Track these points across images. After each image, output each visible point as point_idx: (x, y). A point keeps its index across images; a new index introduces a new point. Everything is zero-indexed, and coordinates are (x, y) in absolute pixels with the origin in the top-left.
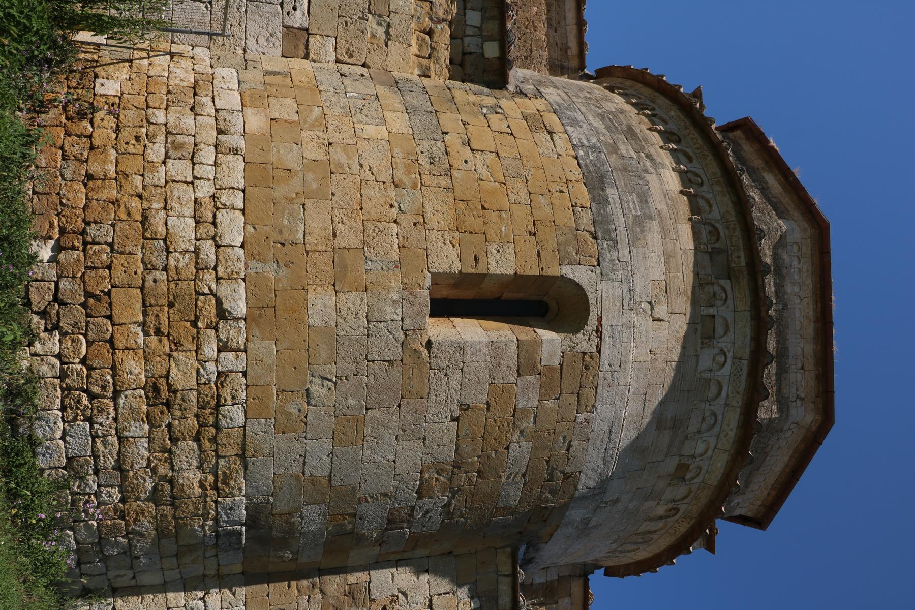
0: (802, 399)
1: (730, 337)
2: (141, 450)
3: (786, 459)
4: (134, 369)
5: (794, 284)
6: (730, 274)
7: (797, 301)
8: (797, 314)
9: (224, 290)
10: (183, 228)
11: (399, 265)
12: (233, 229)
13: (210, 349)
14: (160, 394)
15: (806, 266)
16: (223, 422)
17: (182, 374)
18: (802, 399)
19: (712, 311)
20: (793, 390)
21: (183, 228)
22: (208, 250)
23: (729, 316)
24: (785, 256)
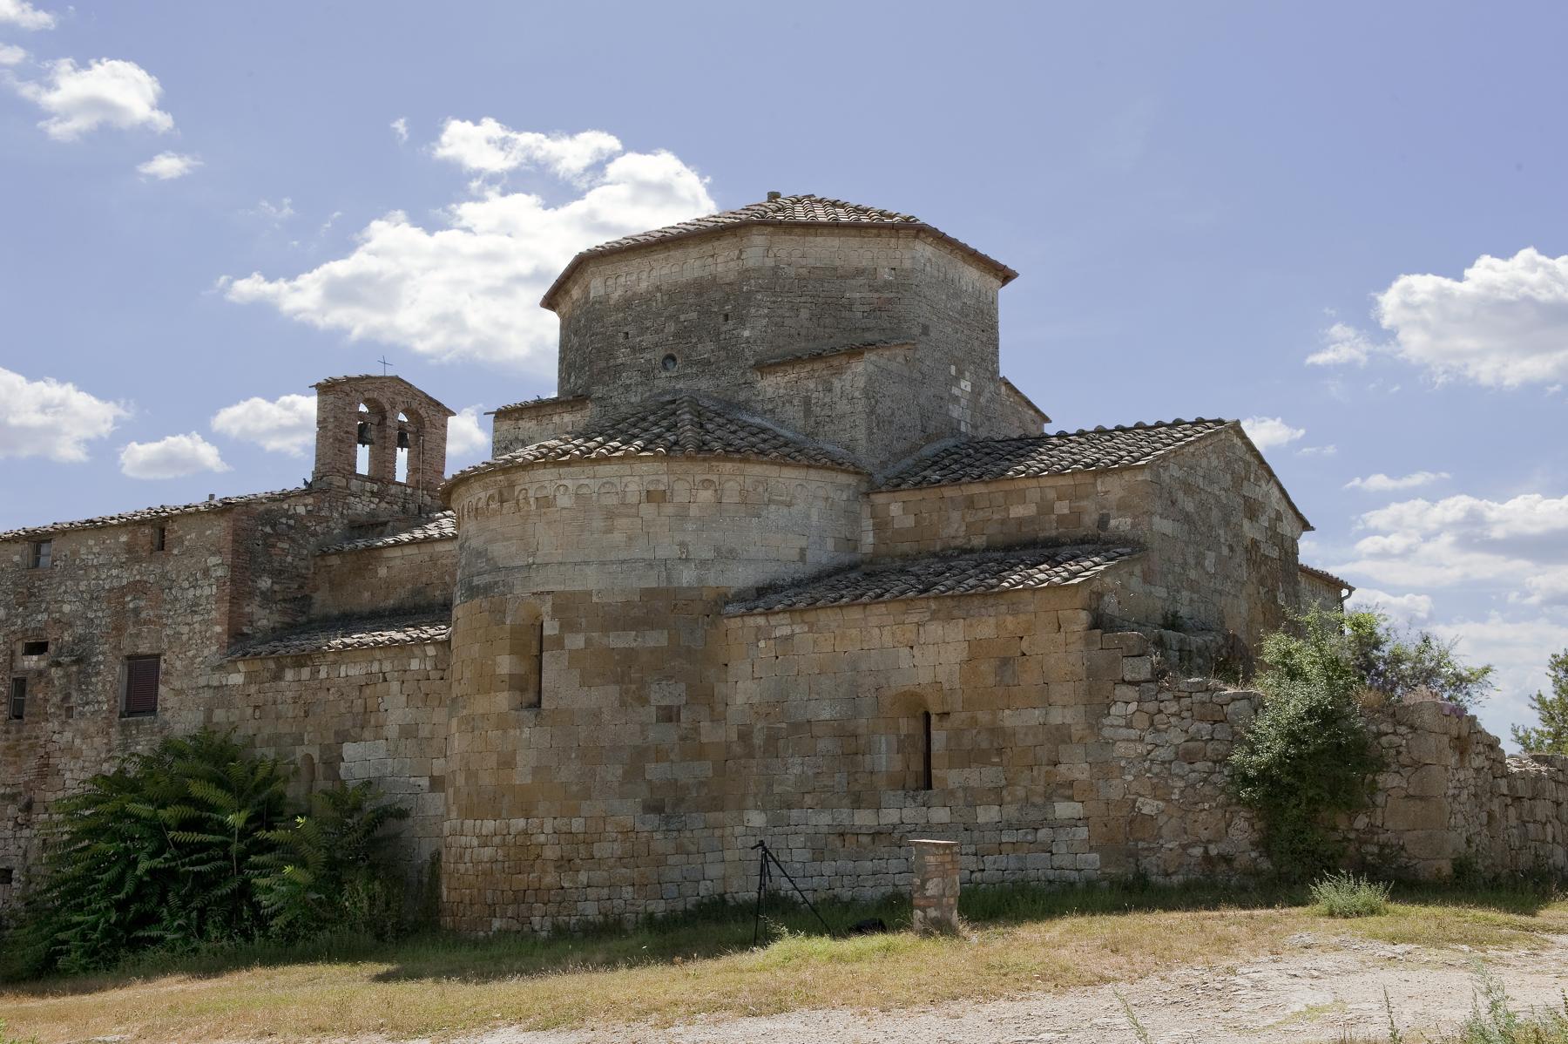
0: (741, 252)
1: (546, 484)
2: (599, 875)
3: (819, 239)
4: (549, 879)
5: (639, 279)
6: (512, 486)
7: (654, 273)
8: (665, 271)
9: (512, 831)
10: (487, 852)
11: (505, 730)
12: (489, 825)
13: (542, 838)
14: (565, 863)
15: (623, 268)
16: (582, 829)
17: (550, 853)
18: (741, 252)
19: (532, 501)
20: (732, 264)
21: (487, 852)
22: (497, 840)
23: (536, 486)
24: (616, 296)
